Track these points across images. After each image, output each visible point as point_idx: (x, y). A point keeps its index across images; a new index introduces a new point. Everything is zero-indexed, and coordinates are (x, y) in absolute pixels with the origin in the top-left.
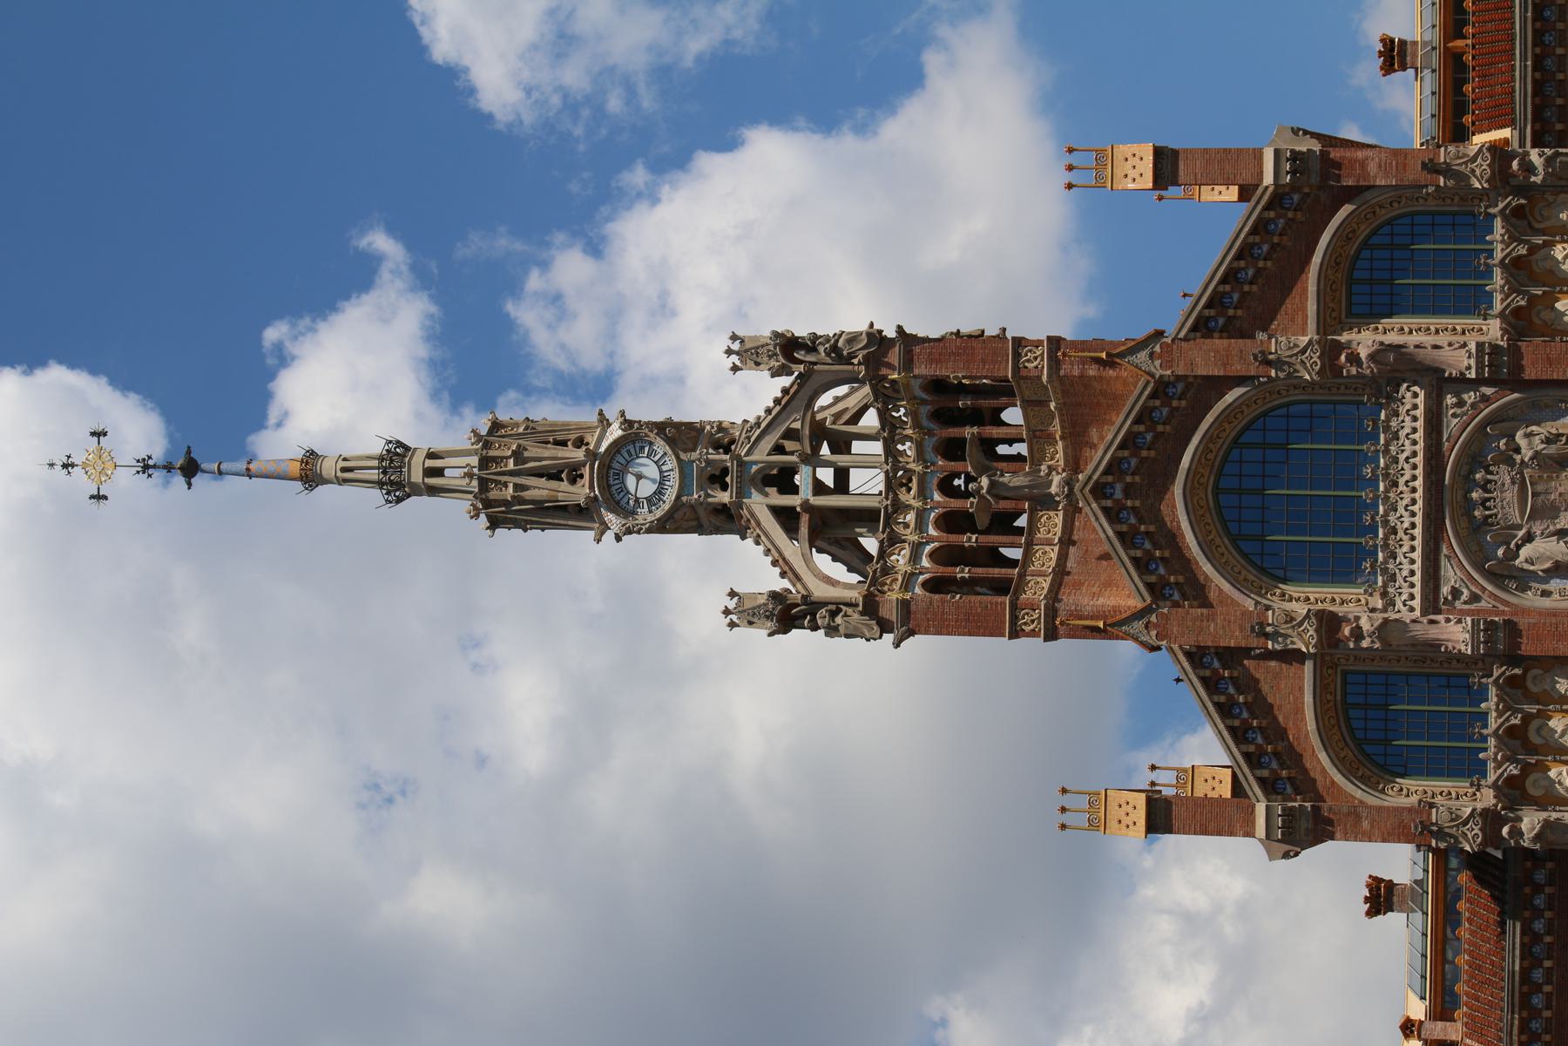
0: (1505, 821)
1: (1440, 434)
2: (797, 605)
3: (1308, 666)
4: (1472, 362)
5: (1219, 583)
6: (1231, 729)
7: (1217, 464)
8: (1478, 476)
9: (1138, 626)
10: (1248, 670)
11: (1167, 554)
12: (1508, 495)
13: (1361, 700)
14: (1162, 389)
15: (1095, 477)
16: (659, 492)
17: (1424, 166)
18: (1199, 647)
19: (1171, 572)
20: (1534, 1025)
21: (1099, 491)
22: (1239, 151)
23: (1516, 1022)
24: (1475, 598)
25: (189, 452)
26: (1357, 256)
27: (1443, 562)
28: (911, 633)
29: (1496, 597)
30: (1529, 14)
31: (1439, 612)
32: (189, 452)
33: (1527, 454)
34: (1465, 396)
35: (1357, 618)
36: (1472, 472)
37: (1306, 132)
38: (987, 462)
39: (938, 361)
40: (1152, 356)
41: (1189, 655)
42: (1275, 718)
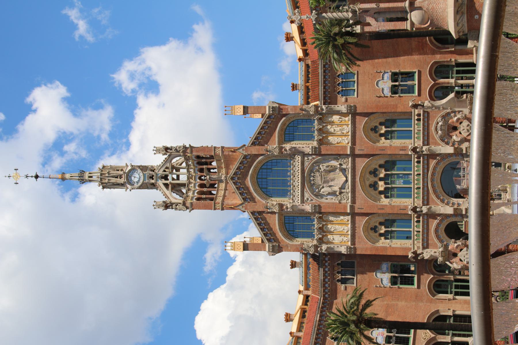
0: (319, 247)
1: (304, 166)
2: (169, 204)
3: (277, 215)
4: (311, 150)
5: (257, 198)
6: (261, 229)
8: (312, 174)
9: (241, 207)
10: (264, 216)
11: (247, 192)
12: (318, 178)
13: (288, 222)
14: (245, 157)
15: (231, 176)
16: (139, 180)
17: (300, 109)
18: (253, 211)
19: (248, 195)
20: (326, 291)
21: (232, 179)
22: (261, 107)
23: (322, 290)
24: (312, 200)
25: (36, 173)
26: (286, 129)
27: (305, 192)
28: (193, 209)
29: (316, 200)
30: (323, 77)
31: (304, 203)
32: (36, 173)
33: (322, 170)
34: (309, 158)
35: (287, 205)
36: (311, 174)
37: (275, 102)
38: (209, 173)
39: (198, 152)
40: (243, 150)
41: (252, 213)
42: (270, 226)
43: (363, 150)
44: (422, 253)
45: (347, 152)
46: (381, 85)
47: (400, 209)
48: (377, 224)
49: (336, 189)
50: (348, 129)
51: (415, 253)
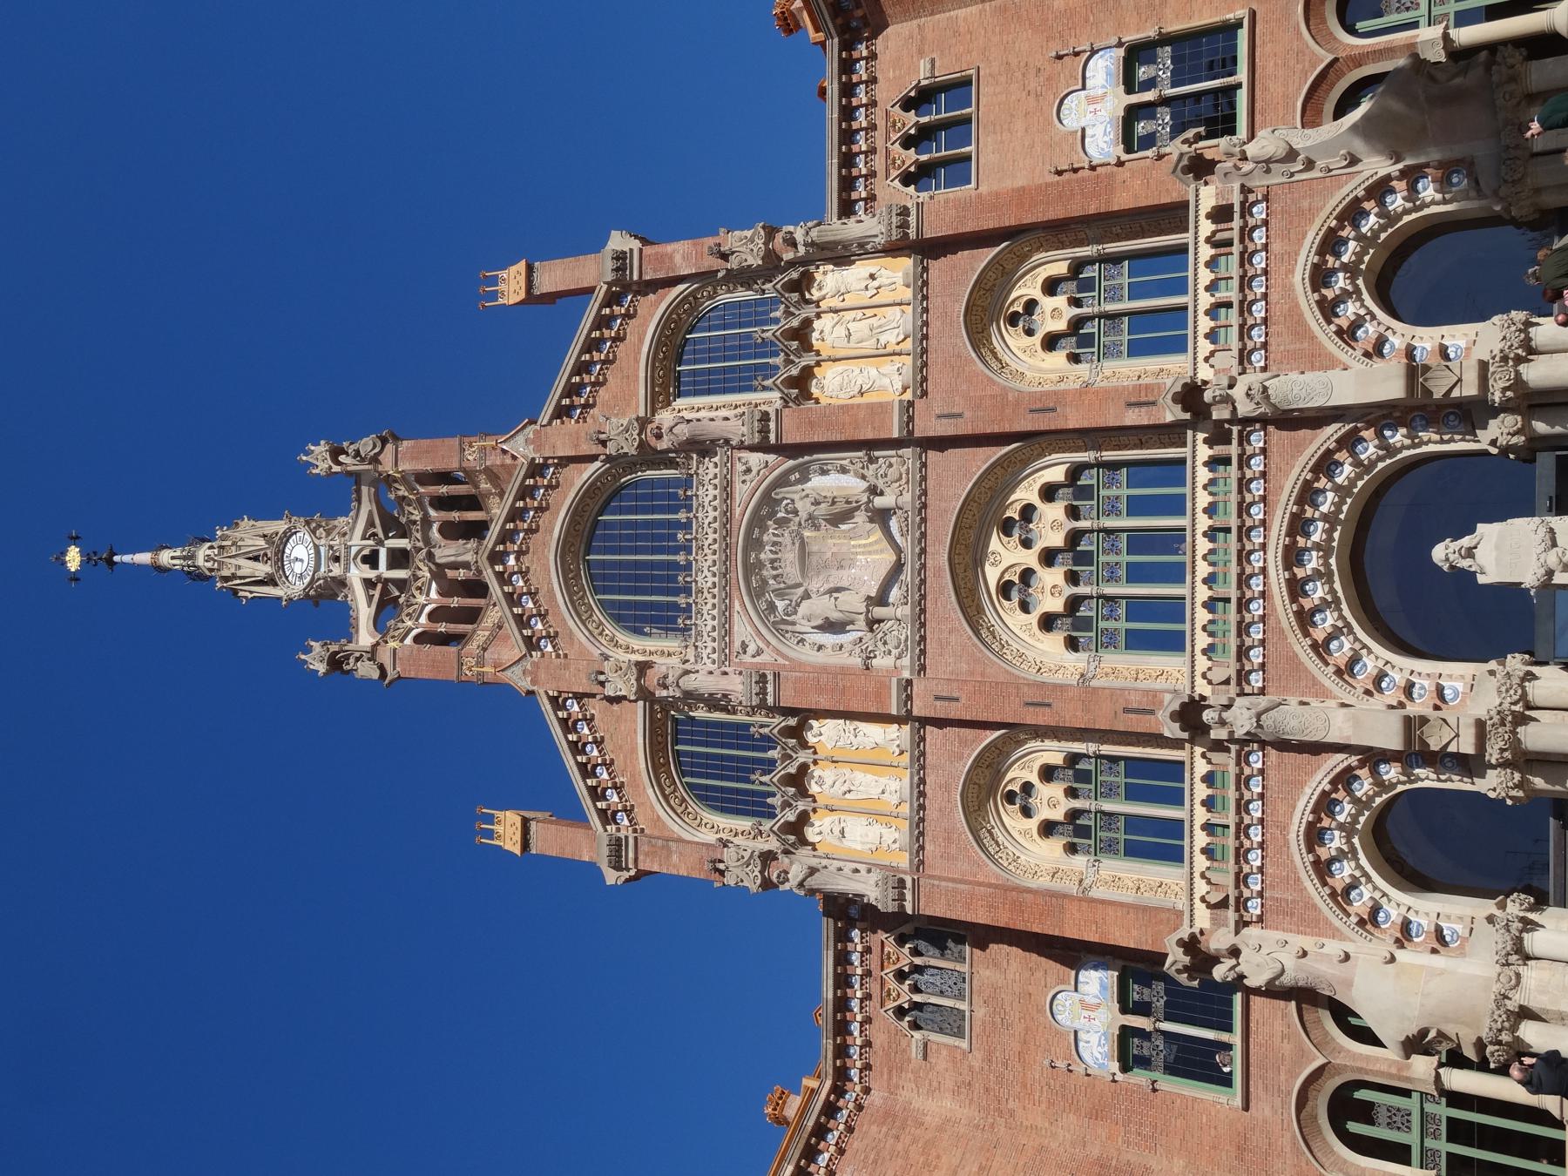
4: (744, 429)
5: (580, 636)
7: (586, 534)
14: (536, 470)
18: (560, 692)
24: (759, 652)
33: (803, 515)
39: (417, 458)
41: (554, 701)
43: (960, 415)
44: (1235, 952)
45: (891, 431)
46: (1076, 113)
47: (1127, 710)
48: (1034, 778)
49: (853, 602)
50: (896, 325)
51: (1191, 945)
